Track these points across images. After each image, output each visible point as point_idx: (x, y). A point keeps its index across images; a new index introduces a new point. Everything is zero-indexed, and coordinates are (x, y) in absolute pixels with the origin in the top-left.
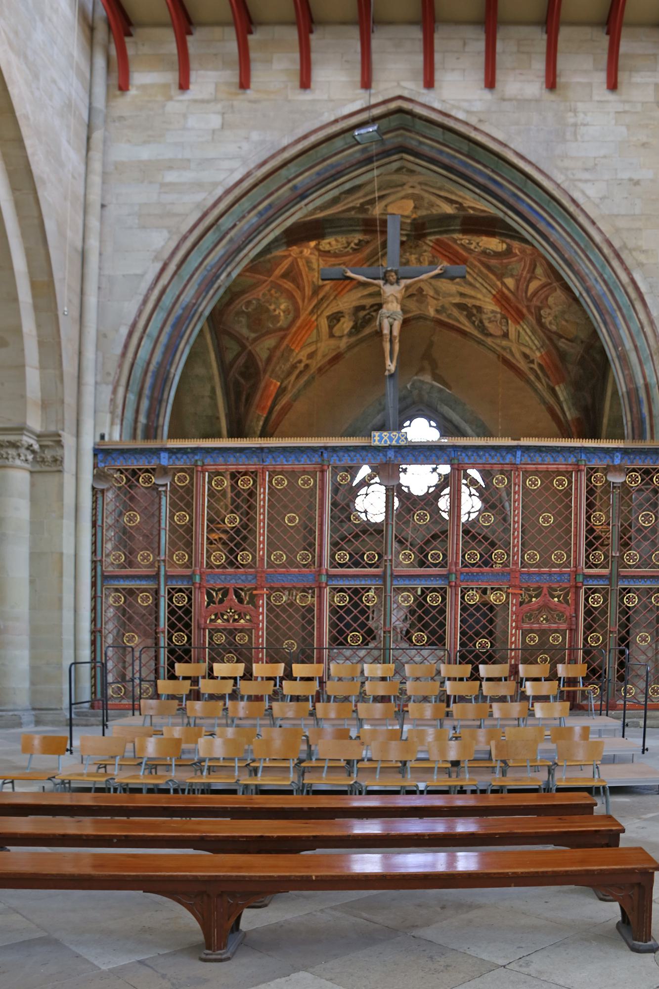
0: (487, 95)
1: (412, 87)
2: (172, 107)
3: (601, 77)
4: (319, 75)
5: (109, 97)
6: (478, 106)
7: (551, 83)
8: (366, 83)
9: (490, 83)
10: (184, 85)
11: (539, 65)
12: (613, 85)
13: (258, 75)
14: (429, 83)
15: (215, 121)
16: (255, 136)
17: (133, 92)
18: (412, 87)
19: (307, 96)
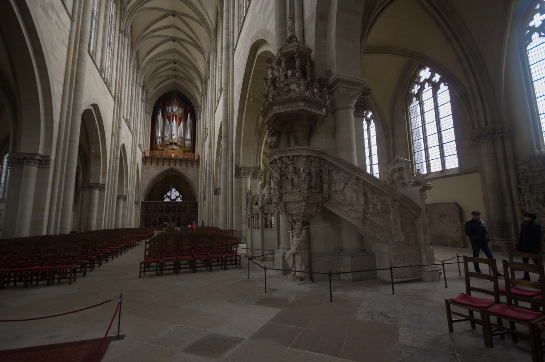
0: (180, 167)
1: (173, 166)
2: (150, 167)
3: (191, 166)
4: (165, 164)
5: (144, 165)
6: (180, 168)
7: (187, 166)
8: (169, 165)
9: (181, 166)
10: (151, 165)
11: (185, 164)
12: (192, 167)
13: (159, 164)
14: (175, 166)
15: (154, 169)
16: (158, 170)
17: (146, 165)
18: (173, 166)
19: (163, 167)
